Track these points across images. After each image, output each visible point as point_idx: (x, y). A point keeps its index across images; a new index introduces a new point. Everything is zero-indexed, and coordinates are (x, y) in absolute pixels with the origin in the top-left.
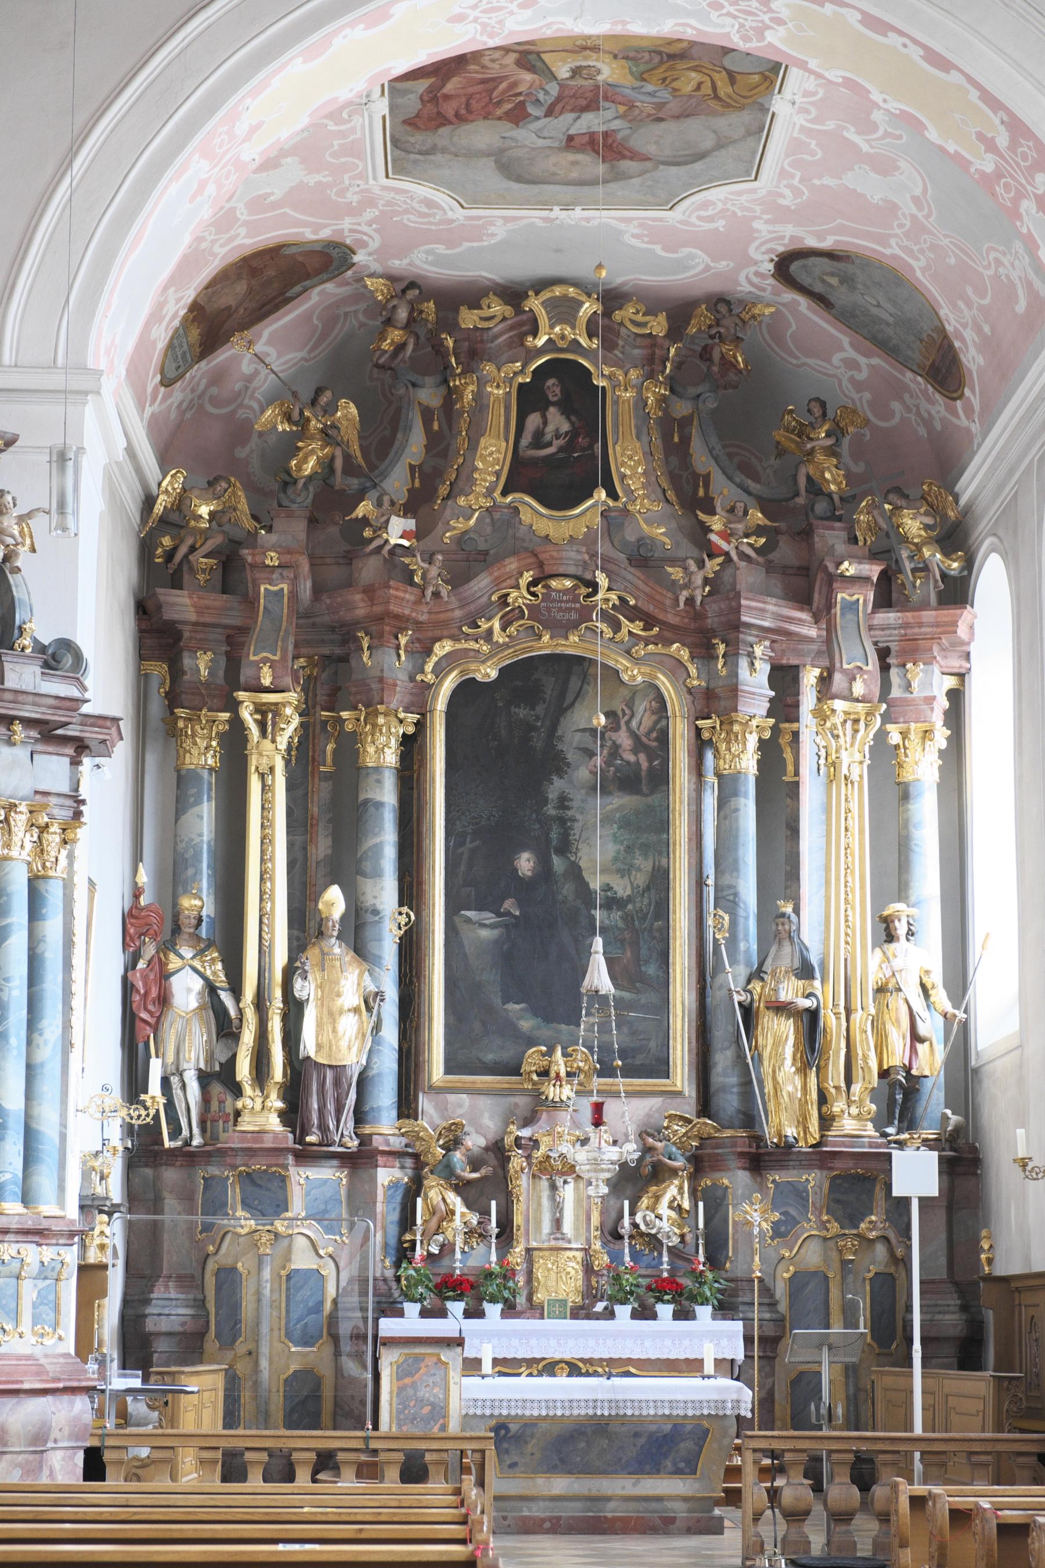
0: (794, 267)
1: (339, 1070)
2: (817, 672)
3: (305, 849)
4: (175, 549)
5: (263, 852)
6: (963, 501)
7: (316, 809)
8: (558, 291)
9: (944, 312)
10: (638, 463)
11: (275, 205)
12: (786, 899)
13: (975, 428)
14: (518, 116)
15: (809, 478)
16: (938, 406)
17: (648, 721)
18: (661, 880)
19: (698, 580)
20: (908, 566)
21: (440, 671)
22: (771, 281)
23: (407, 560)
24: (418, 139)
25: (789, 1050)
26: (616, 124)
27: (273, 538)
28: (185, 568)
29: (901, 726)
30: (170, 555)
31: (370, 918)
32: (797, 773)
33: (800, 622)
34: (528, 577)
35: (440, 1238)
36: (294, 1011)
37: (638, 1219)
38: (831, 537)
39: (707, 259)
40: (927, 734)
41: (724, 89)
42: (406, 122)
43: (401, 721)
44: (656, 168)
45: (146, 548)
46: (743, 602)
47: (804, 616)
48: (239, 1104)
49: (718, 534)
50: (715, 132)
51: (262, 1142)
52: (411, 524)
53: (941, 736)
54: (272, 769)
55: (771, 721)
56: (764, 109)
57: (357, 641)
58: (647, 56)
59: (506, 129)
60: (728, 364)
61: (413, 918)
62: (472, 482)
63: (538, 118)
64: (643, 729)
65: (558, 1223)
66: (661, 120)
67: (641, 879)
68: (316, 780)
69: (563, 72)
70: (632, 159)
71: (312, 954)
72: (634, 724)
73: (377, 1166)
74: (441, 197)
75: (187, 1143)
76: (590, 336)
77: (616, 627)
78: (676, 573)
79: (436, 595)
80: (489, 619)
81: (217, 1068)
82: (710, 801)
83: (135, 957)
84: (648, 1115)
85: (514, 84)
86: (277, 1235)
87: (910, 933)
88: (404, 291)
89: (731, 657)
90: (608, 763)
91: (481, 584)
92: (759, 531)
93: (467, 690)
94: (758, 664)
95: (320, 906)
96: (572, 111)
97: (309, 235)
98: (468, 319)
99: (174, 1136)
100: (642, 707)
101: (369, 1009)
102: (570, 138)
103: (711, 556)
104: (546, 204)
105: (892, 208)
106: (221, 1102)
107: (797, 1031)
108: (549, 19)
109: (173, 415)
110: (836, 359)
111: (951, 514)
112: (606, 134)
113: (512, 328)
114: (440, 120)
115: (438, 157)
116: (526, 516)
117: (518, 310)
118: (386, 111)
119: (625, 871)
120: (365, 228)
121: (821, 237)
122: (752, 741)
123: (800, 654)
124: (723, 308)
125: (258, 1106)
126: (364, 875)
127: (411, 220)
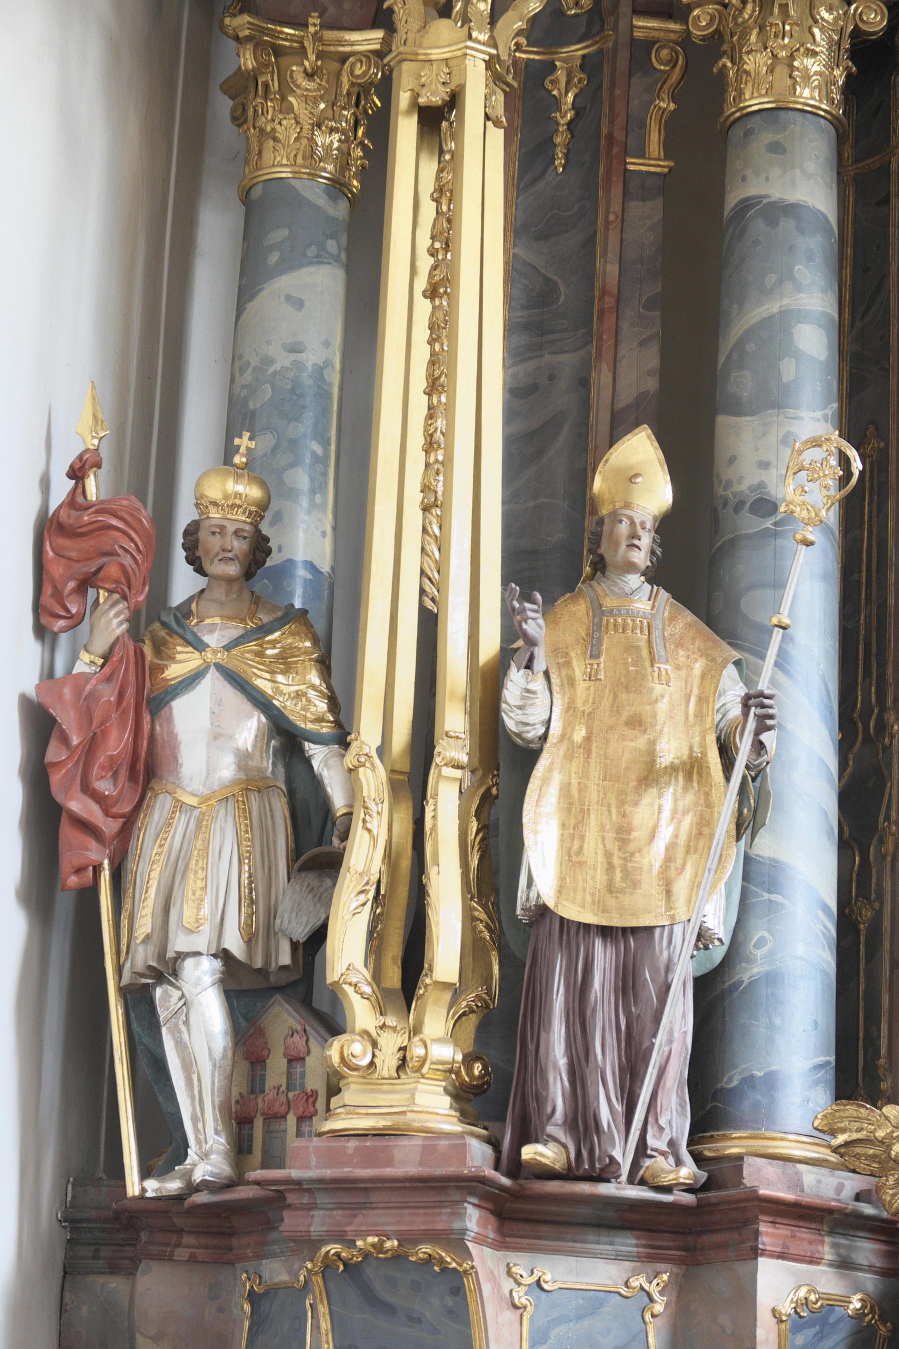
3: (584, 382)
7: (613, 269)
48: (334, 1054)
51: (390, 1162)
54: (455, 100)
61: (857, 465)
68: (617, 191)
73: (755, 1253)
81: (285, 959)
95: (598, 484)
106: (295, 1060)
125: (388, 1061)
126: (736, 408)
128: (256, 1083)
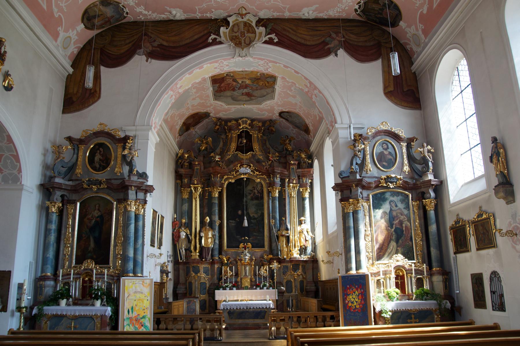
0: (282, 114)
1: (208, 248)
2: (288, 180)
4: (181, 162)
5: (195, 211)
6: (311, 151)
8: (244, 119)
9: (306, 121)
10: (257, 146)
11: (196, 106)
12: (284, 217)
13: (312, 139)
14: (234, 90)
15: (286, 148)
16: (306, 136)
17: (260, 188)
18: (262, 215)
19: (267, 164)
20: (302, 162)
21: (225, 181)
22: (278, 117)
23: (219, 163)
24: (218, 94)
25: (284, 243)
26: (250, 91)
27: (197, 160)
28: (183, 165)
29: (302, 188)
30: (180, 163)
31: (213, 222)
32: (285, 196)
33: (285, 171)
34: (239, 165)
35: (226, 277)
36: (201, 238)
37: (260, 272)
38: (290, 158)
40: (307, 189)
41: (267, 84)
42: (216, 91)
43: (219, 189)
44: (257, 98)
45: (177, 162)
46: (275, 168)
47: (285, 170)
49: (271, 157)
50: (266, 92)
52: (220, 157)
53: (309, 190)
54: (197, 198)
55: (280, 188)
56: (274, 88)
57: (211, 176)
59: (232, 92)
60: (272, 130)
62: (230, 150)
64: (259, 190)
65: (246, 273)
66: (257, 90)
67: (259, 215)
69: (240, 82)
70: (253, 96)
71: (204, 229)
72: (258, 189)
73: (215, 264)
74: (223, 104)
75: (183, 261)
76: (249, 126)
77: (254, 173)
78: (264, 164)
79: (224, 168)
80: (233, 172)
82: (271, 202)
83: (175, 229)
84: (261, 255)
85: (232, 84)
86: (198, 276)
87: (305, 223)
88: (219, 120)
89: (273, 178)
90: (254, 195)
91: (232, 166)
92: (278, 157)
93: (230, 184)
94: (278, 178)
97: (202, 111)
98: (229, 124)
99: (181, 260)
100: (259, 186)
101: (213, 238)
102: (243, 93)
103: (269, 161)
104: (240, 104)
105: (296, 104)
106: (189, 254)
107: (286, 240)
108: (231, 68)
109: (182, 140)
110: (290, 129)
111: (309, 153)
112: (248, 93)
113: (237, 125)
114: (221, 91)
115: (222, 97)
116: (239, 155)
117: (237, 122)
119: (257, 213)
120: (211, 110)
121: (286, 109)
122: (277, 191)
123: (284, 176)
124: (271, 122)
125: (195, 255)
126: (213, 215)
127: (218, 108)
128: (187, 255)
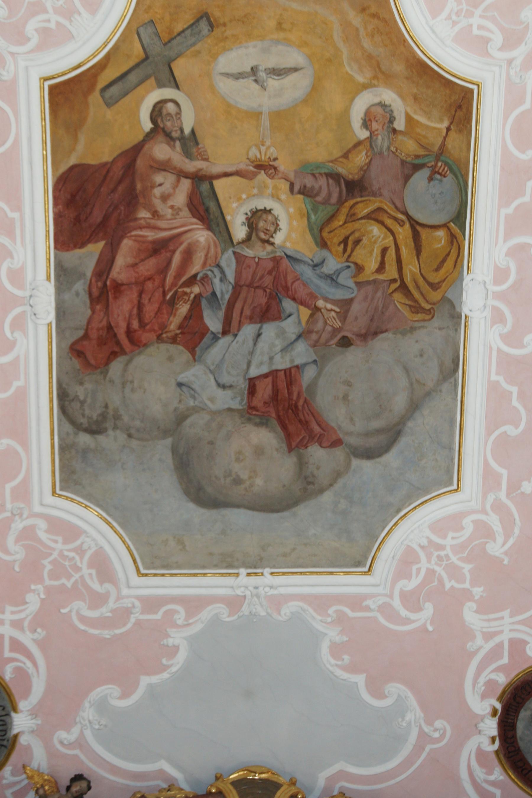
39: (420, 714)
58: (323, 182)
63: (215, 338)
96: (251, 319)
118: (52, 317)
